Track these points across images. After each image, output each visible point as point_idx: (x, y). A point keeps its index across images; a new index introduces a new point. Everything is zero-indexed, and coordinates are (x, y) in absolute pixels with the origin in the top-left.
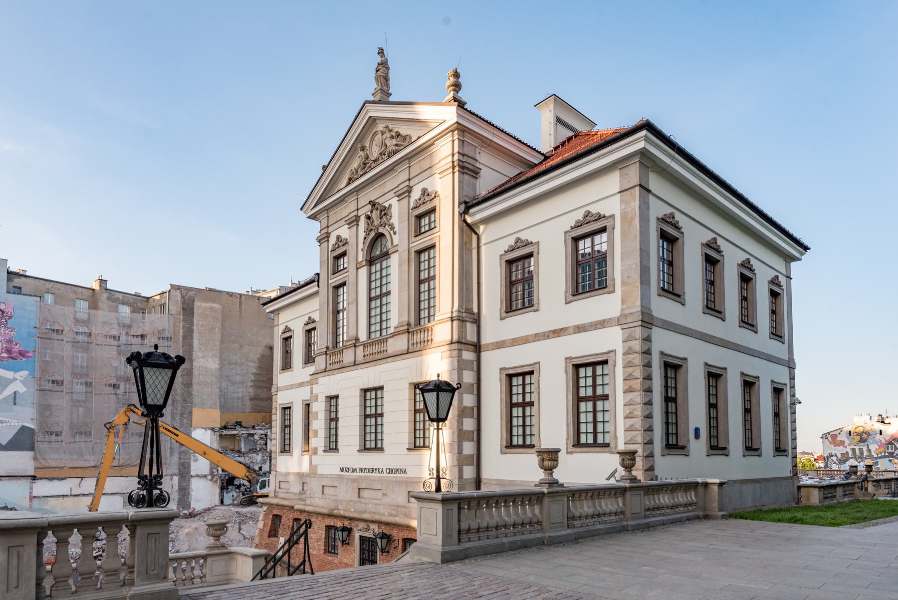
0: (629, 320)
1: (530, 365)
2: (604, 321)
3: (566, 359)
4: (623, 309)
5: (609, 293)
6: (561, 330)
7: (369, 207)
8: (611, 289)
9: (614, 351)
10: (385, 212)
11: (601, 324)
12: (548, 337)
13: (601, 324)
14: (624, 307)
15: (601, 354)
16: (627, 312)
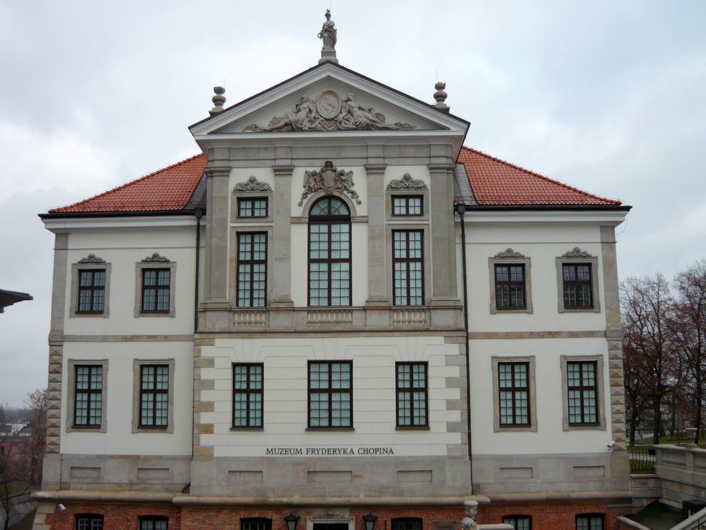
0: (614, 335)
1: (526, 357)
2: (594, 332)
3: (562, 356)
4: (607, 326)
5: (595, 312)
6: (556, 333)
7: (323, 163)
8: (598, 310)
9: (602, 356)
10: (343, 179)
11: (591, 334)
12: (543, 337)
13: (591, 334)
14: (609, 325)
15: (593, 356)
16: (613, 329)
